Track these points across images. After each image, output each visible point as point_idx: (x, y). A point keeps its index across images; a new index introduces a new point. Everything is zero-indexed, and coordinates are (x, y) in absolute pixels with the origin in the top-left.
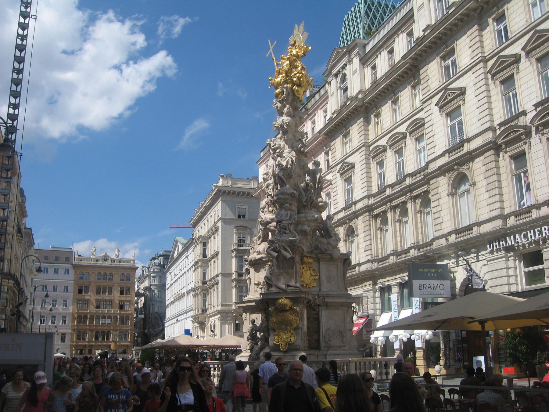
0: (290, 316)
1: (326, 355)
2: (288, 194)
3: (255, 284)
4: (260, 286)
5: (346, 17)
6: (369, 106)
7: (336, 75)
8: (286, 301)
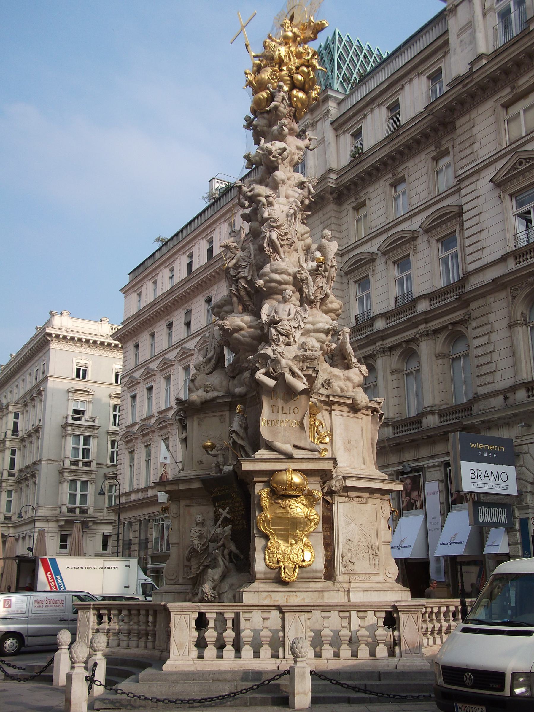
1: (349, 591)
2: (290, 274)
8: (297, 479)
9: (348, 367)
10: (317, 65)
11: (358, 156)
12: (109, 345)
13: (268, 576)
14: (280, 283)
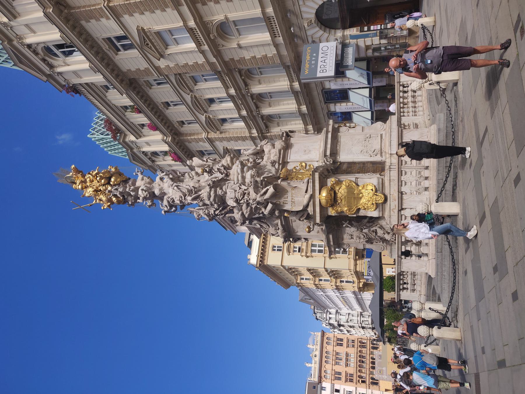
0: (342, 191)
2: (210, 190)
3: (309, 232)
4: (311, 227)
5: (109, 153)
6: (173, 132)
7: (153, 161)
9: (263, 151)
10: (95, 172)
11: (154, 128)
12: (264, 238)
13: (381, 209)
14: (216, 195)
